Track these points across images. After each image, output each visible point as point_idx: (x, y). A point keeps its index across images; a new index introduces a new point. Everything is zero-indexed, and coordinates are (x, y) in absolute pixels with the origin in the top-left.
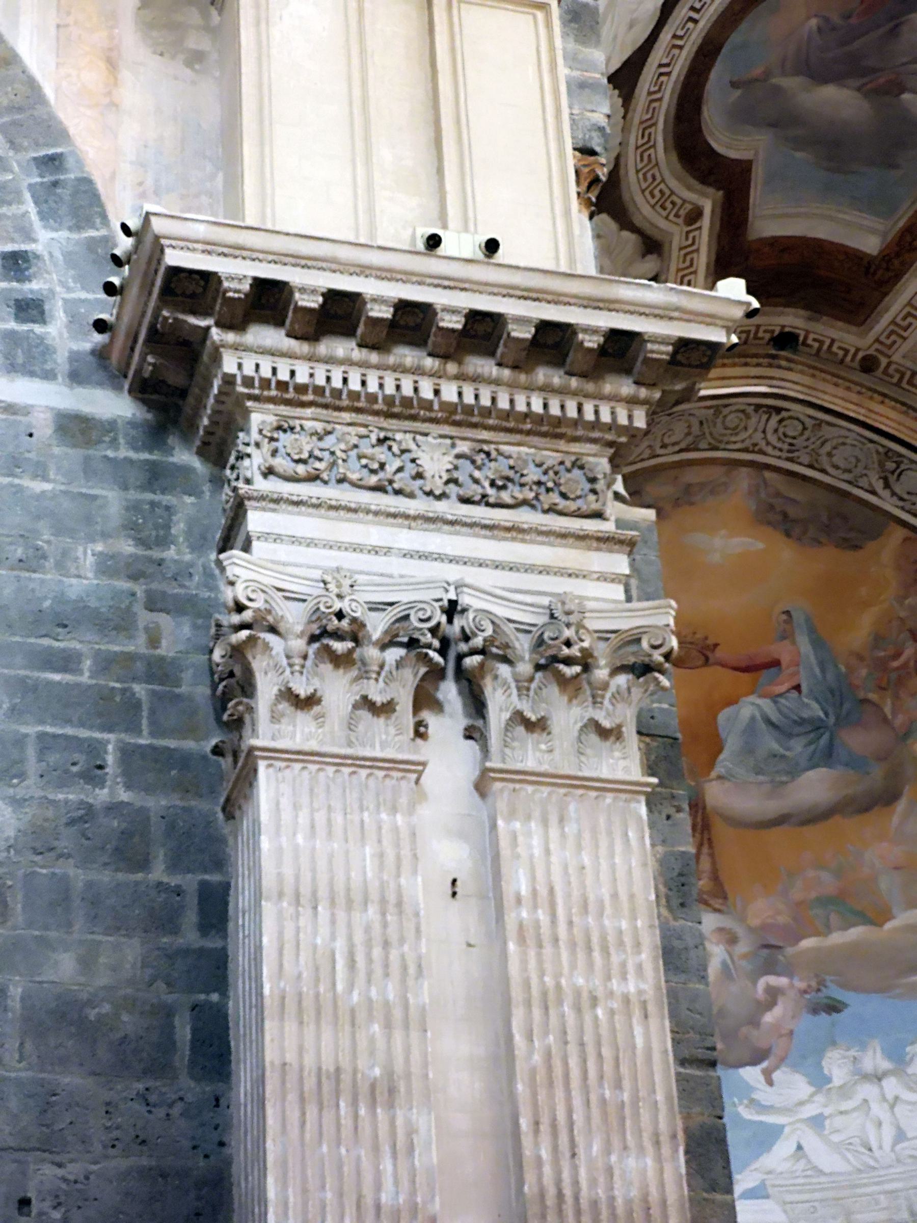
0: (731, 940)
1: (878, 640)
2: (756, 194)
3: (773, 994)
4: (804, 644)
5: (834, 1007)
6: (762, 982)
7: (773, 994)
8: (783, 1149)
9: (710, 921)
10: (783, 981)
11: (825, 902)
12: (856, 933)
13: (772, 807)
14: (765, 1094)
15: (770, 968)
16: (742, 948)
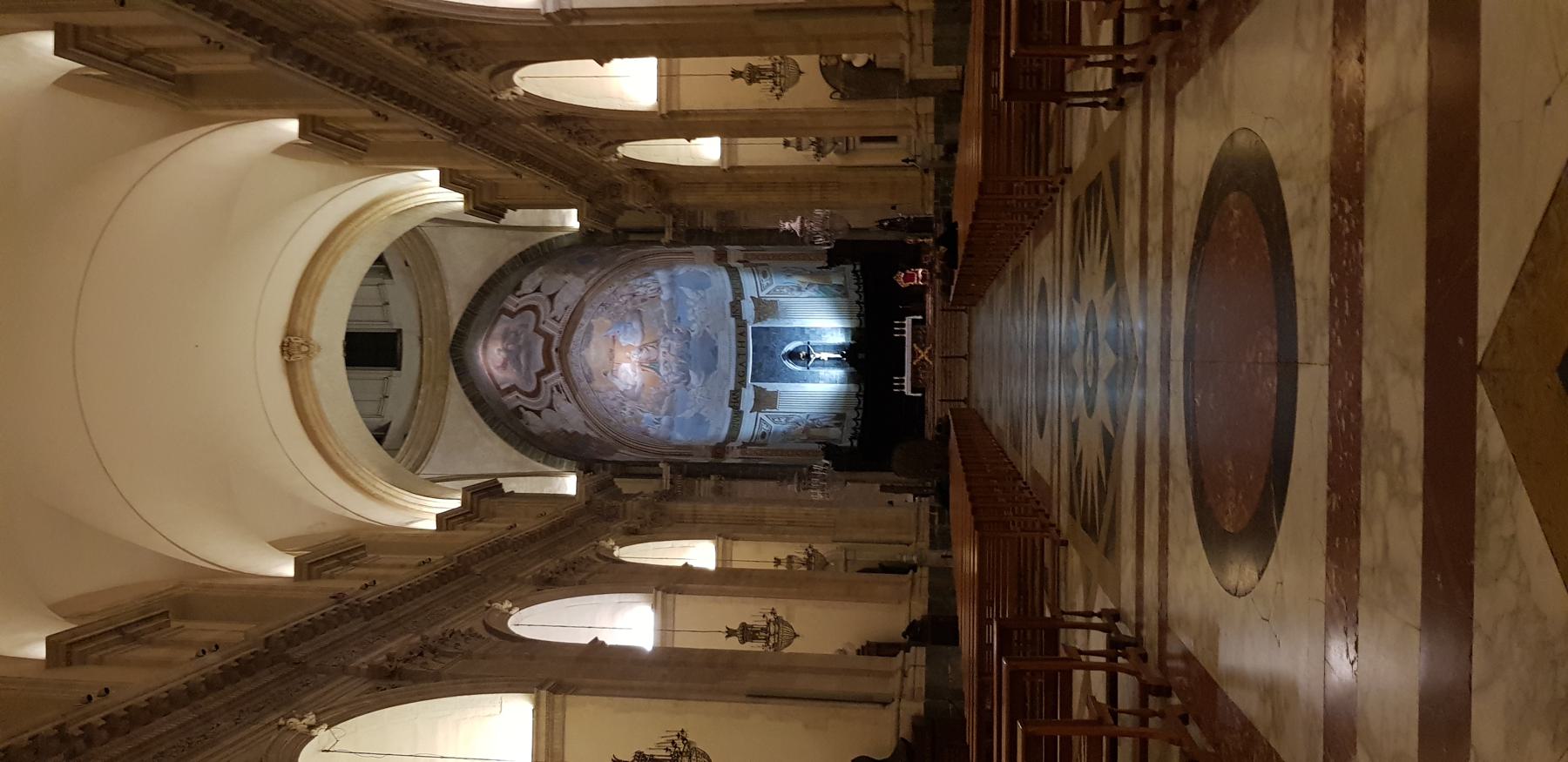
0: (666, 338)
1: (610, 319)
2: (538, 370)
3: (677, 330)
4: (610, 332)
5: (679, 319)
6: (674, 332)
7: (677, 330)
8: (707, 329)
9: (662, 343)
10: (674, 330)
11: (658, 321)
12: (665, 315)
13: (640, 333)
14: (696, 333)
15: (671, 331)
16: (667, 336)
